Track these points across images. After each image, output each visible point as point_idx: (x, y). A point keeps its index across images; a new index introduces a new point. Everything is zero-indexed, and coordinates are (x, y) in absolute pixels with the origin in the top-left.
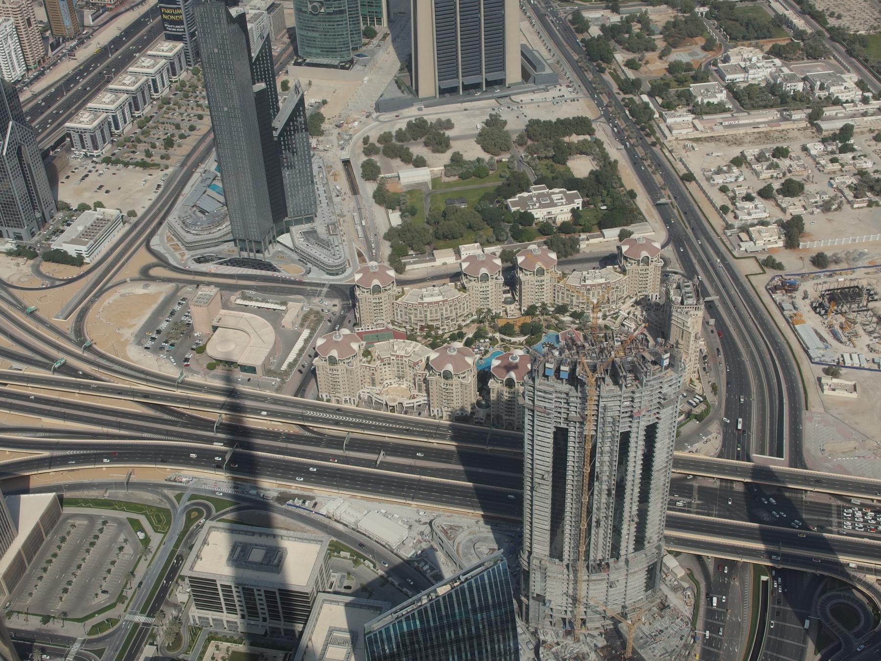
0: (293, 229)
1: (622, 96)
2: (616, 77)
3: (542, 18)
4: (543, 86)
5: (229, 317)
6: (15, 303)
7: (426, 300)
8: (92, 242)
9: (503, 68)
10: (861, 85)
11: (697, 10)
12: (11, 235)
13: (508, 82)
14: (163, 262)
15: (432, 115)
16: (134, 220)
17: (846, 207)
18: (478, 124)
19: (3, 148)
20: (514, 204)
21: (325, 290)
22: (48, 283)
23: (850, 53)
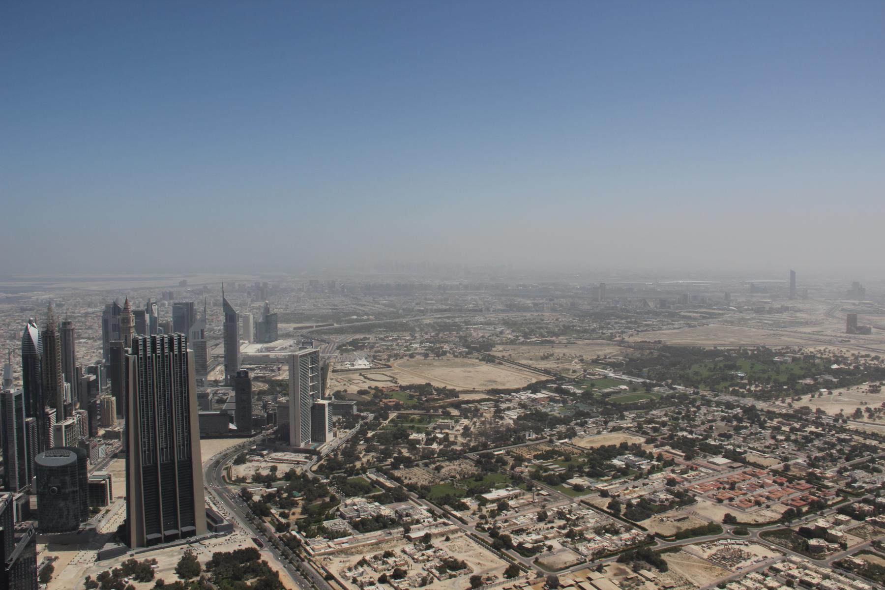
1: (277, 535)
2: (272, 523)
3: (220, 495)
4: (223, 533)
9: (194, 524)
10: (430, 511)
11: (322, 481)
15: (141, 558)
17: (436, 580)
23: (422, 497)
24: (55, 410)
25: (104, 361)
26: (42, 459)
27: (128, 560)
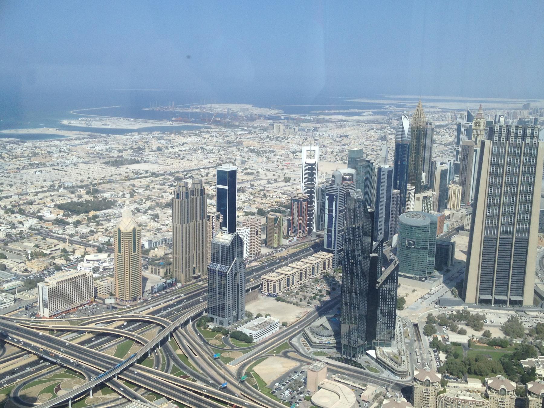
0: (377, 348)
5: (329, 384)
6: (209, 353)
7: (461, 397)
8: (259, 331)
9: (522, 296)
12: (218, 321)
13: (524, 304)
14: (298, 351)
15: (473, 311)
16: (285, 328)
18: (504, 320)
19: (228, 270)
20: (526, 363)
21: (392, 385)
22: (230, 348)
24: (414, 187)
25: (454, 159)
26: (403, 218)
27: (463, 310)
